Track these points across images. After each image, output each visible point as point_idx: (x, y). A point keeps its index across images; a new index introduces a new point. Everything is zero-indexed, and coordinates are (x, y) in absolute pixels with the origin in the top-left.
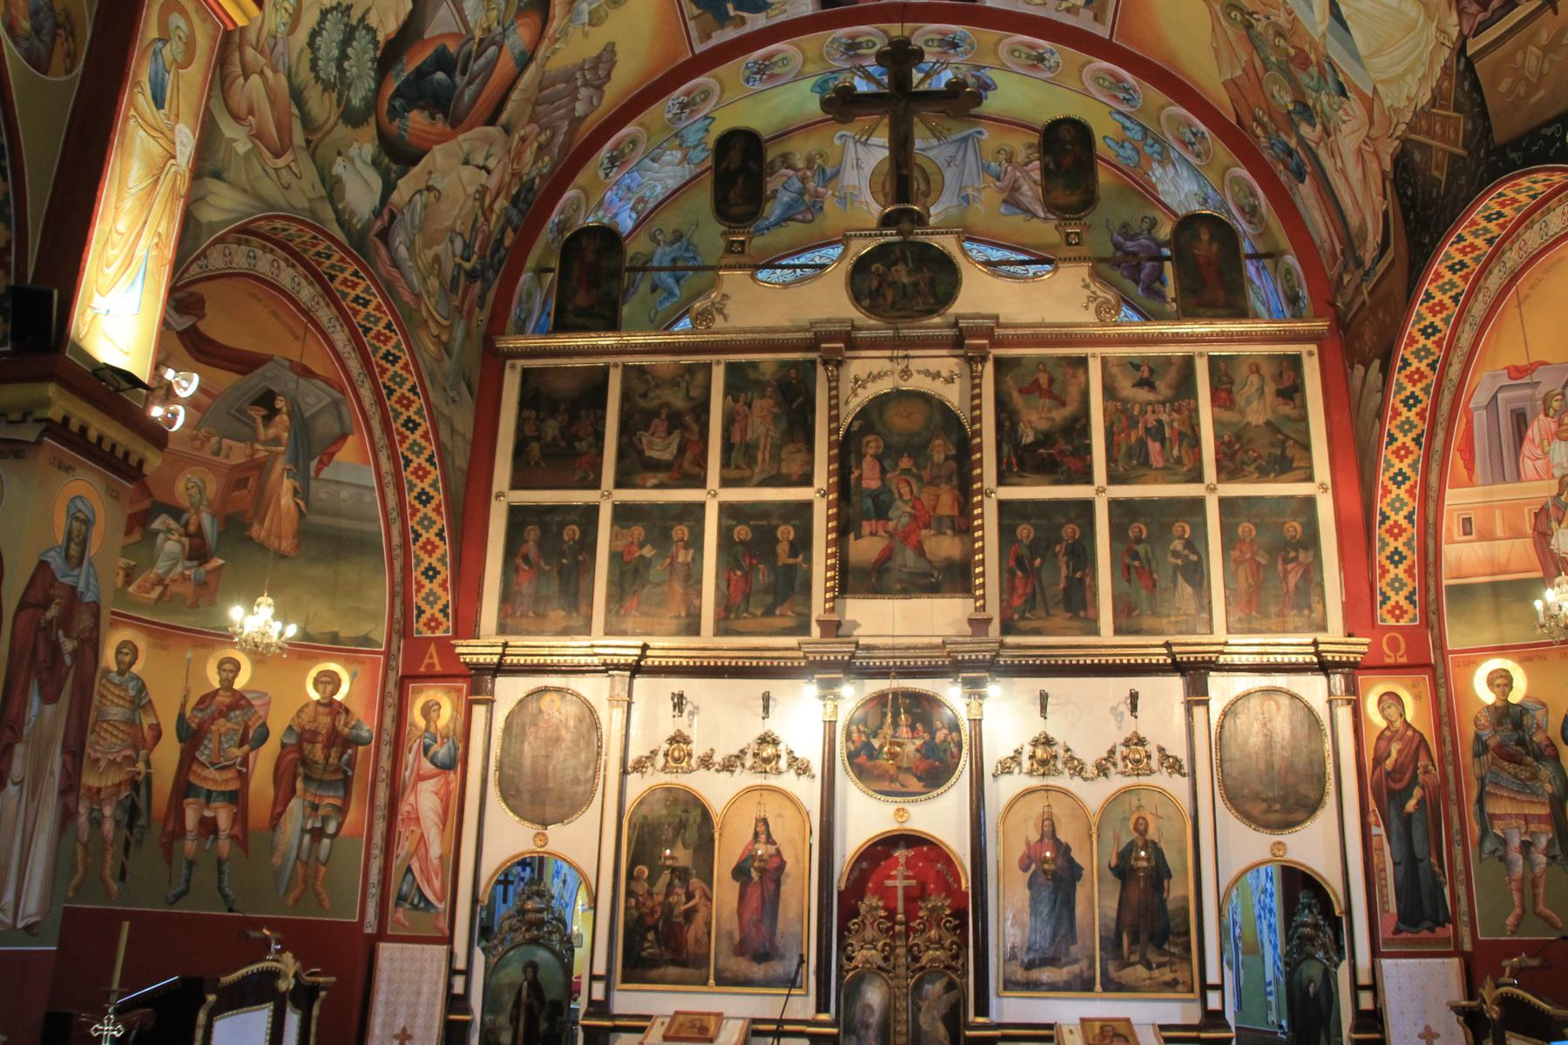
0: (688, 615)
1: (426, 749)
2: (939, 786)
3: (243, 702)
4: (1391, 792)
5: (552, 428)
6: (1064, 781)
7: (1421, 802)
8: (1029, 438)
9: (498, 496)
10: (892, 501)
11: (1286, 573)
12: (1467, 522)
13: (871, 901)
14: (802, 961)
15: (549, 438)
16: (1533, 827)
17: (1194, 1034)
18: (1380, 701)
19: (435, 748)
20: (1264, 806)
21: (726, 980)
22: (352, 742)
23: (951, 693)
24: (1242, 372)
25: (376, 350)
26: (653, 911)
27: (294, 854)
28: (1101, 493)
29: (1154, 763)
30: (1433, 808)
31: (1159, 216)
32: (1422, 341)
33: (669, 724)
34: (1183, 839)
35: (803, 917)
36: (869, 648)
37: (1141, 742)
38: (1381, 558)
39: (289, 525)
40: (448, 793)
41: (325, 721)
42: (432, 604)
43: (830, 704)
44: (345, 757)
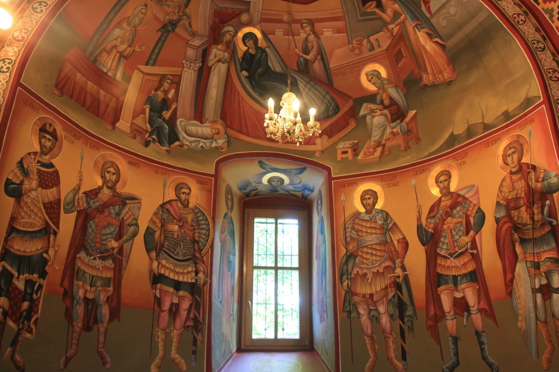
3: (460, 199)
27: (532, 315)
39: (441, 60)
41: (521, 185)
44: (546, 209)
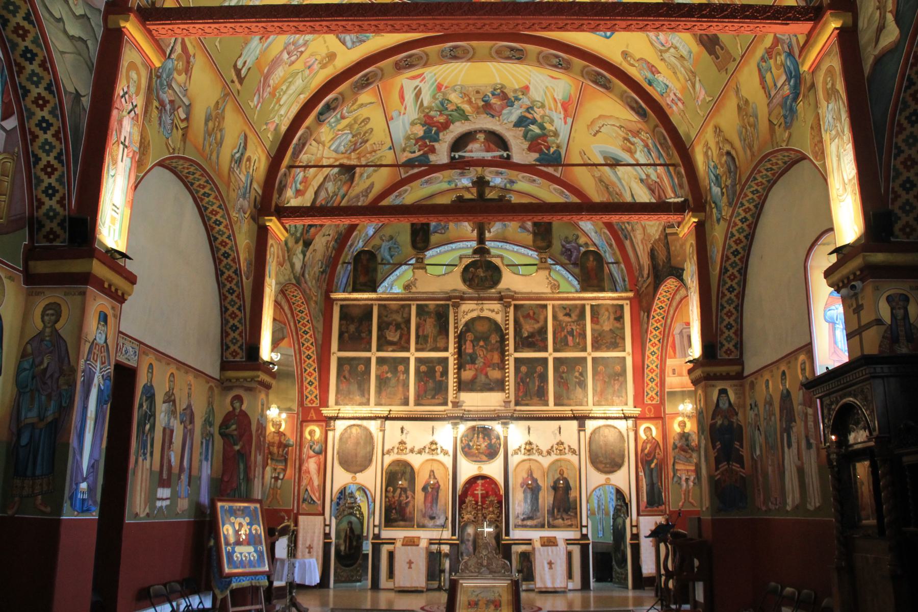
0: (405, 398)
1: (311, 447)
2: (493, 458)
4: (646, 461)
5: (352, 328)
6: (536, 457)
8: (526, 335)
9: (334, 353)
10: (477, 358)
11: (614, 384)
12: (674, 370)
14: (447, 519)
16: (689, 473)
18: (645, 430)
19: (314, 446)
21: (422, 526)
22: (287, 446)
23: (497, 427)
24: (602, 311)
25: (296, 309)
26: (394, 503)
28: (550, 355)
29: (567, 451)
31: (580, 234)
32: (659, 311)
33: (399, 437)
34: (576, 477)
35: (446, 504)
36: (468, 411)
37: (562, 444)
38: (646, 380)
41: (277, 439)
42: (311, 395)
43: (455, 431)
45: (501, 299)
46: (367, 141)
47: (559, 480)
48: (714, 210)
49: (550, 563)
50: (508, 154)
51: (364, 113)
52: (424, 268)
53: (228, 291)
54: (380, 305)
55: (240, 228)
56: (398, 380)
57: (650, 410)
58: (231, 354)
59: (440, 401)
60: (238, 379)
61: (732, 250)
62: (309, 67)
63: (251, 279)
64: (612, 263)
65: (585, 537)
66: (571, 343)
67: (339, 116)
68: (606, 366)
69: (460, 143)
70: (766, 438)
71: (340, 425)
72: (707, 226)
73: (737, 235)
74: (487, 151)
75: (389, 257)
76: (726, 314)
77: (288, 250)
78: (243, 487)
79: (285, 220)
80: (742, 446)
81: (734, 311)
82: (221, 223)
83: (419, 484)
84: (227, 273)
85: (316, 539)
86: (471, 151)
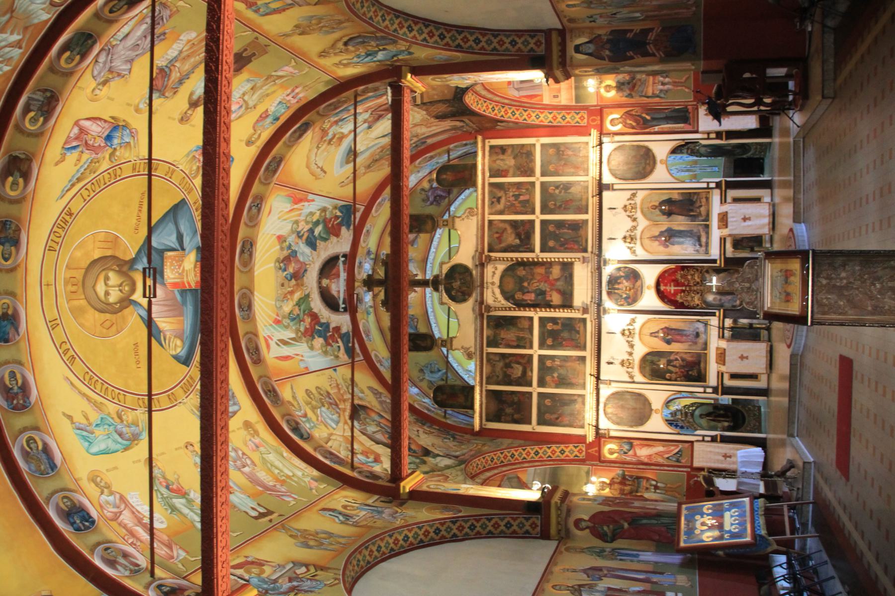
0: (578, 360)
1: (625, 453)
4: (644, 124)
5: (509, 410)
6: (638, 233)
7: (647, 114)
8: (518, 241)
11: (567, 155)
12: (555, 97)
13: (679, 298)
14: (698, 321)
15: (513, 411)
16: (657, 81)
17: (723, 192)
18: (612, 125)
19: (625, 450)
20: (648, 166)
21: (705, 346)
22: (624, 477)
23: (608, 271)
24: (495, 166)
26: (682, 372)
28: (538, 217)
29: (632, 202)
30: (648, 109)
31: (420, 188)
33: (617, 367)
35: (685, 321)
36: (592, 298)
37: (625, 206)
38: (563, 123)
40: (641, 445)
41: (616, 486)
43: (611, 311)
45: (482, 265)
46: (328, 393)
47: (661, 211)
48: (400, 57)
49: (745, 219)
50: (343, 257)
51: (301, 395)
52: (452, 339)
53: (472, 530)
54: (488, 383)
55: (411, 517)
56: (560, 366)
57: (593, 120)
58: (534, 529)
59: (582, 325)
60: (558, 523)
61: (439, 40)
62: (257, 447)
63: (461, 508)
64: (449, 156)
65: (718, 185)
66: (526, 197)
67: (304, 419)
68: (550, 163)
69: (330, 302)
70: (625, 7)
71: (605, 424)
72: (415, 64)
73: (425, 35)
74: (338, 276)
75: (440, 373)
76: (501, 46)
77: (433, 471)
78: (665, 520)
79: (404, 474)
80: (631, 31)
81: (498, 39)
82: (406, 536)
83: (664, 347)
84: (455, 531)
85: (717, 450)
86: (339, 292)
